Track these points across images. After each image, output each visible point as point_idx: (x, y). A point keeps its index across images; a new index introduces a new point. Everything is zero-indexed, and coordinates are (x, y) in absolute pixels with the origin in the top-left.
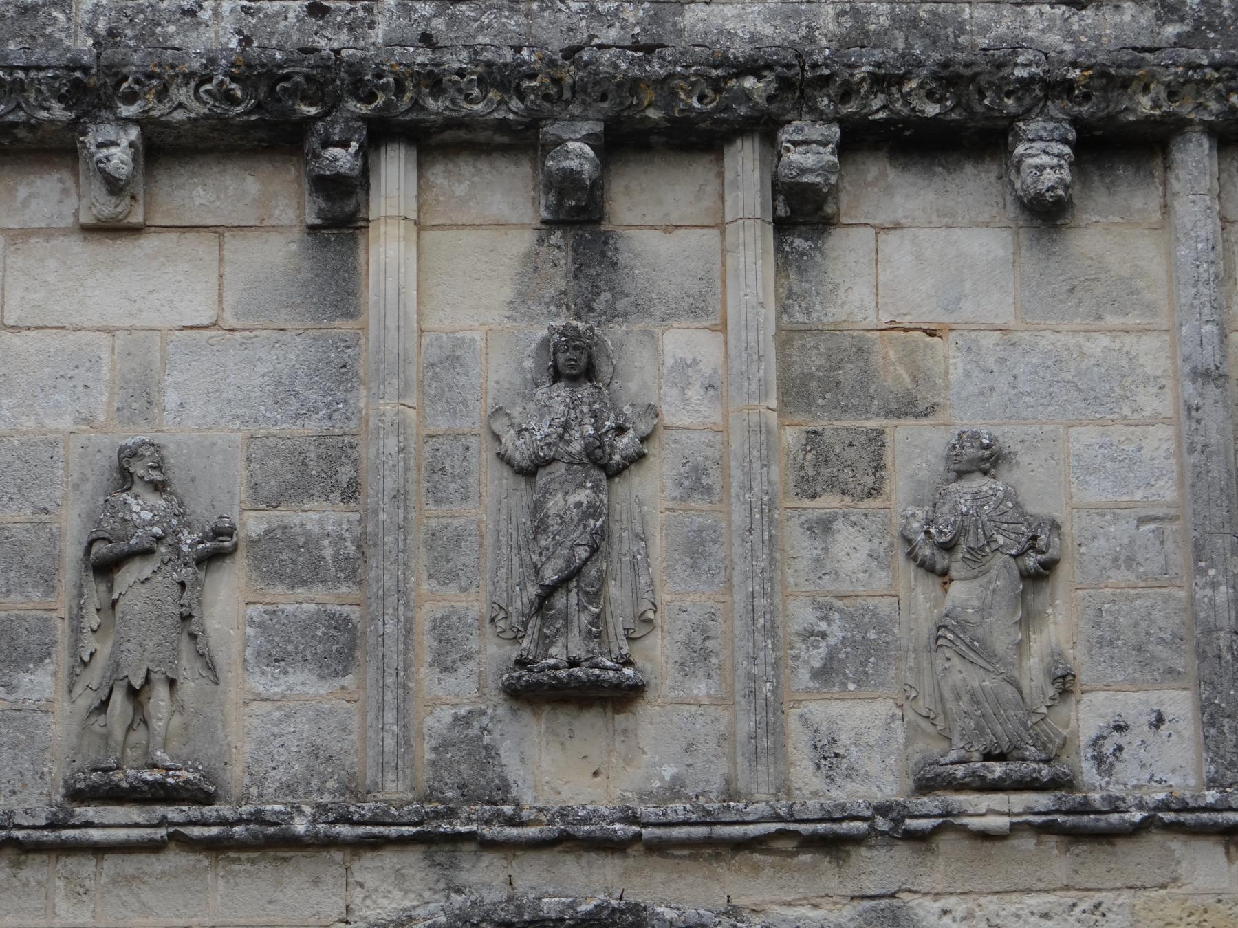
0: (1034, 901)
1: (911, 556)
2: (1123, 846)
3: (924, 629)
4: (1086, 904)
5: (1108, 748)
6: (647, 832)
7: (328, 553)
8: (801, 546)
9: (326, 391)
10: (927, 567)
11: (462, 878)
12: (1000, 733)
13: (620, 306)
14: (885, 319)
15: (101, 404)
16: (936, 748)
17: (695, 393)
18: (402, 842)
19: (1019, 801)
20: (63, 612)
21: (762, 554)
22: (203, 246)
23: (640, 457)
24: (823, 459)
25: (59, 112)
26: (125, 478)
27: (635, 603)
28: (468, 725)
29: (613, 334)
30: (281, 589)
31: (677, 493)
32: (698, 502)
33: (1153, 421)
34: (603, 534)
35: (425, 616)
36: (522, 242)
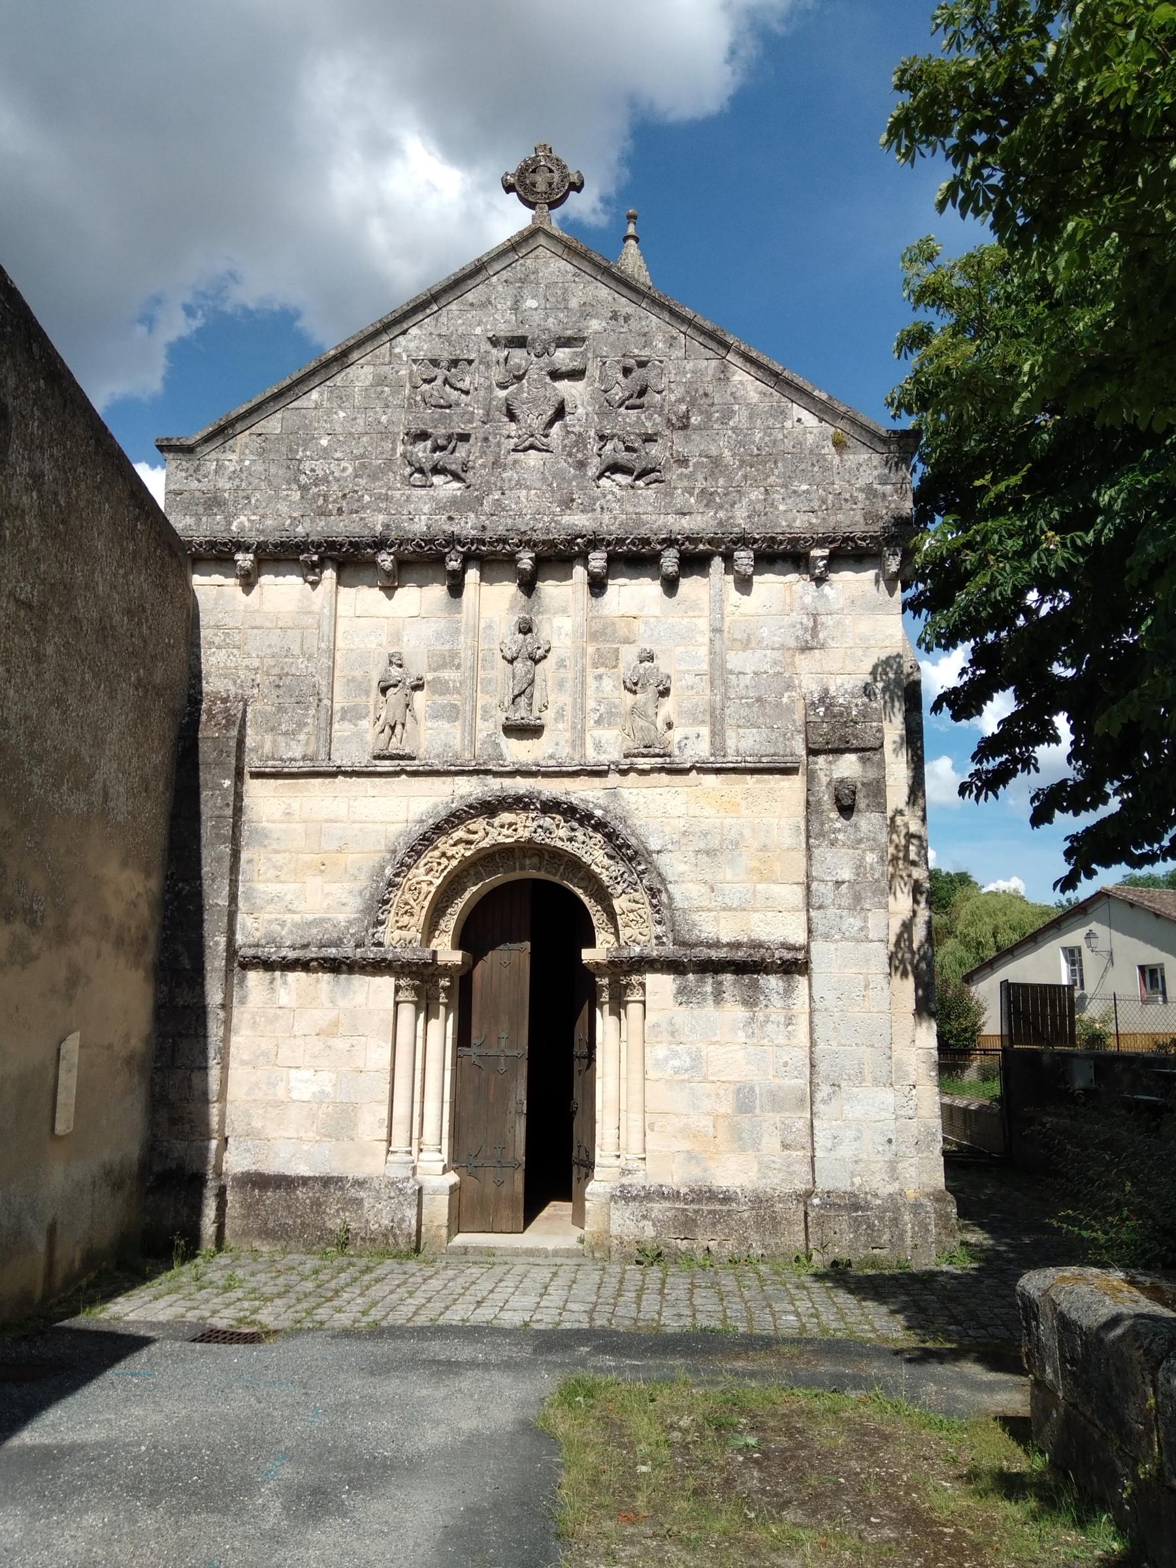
0: (658, 790)
1: (626, 687)
3: (628, 708)
10: (630, 690)
15: (384, 640)
16: (631, 744)
19: (653, 760)
21: (579, 686)
23: (545, 657)
26: (391, 663)
29: (537, 619)
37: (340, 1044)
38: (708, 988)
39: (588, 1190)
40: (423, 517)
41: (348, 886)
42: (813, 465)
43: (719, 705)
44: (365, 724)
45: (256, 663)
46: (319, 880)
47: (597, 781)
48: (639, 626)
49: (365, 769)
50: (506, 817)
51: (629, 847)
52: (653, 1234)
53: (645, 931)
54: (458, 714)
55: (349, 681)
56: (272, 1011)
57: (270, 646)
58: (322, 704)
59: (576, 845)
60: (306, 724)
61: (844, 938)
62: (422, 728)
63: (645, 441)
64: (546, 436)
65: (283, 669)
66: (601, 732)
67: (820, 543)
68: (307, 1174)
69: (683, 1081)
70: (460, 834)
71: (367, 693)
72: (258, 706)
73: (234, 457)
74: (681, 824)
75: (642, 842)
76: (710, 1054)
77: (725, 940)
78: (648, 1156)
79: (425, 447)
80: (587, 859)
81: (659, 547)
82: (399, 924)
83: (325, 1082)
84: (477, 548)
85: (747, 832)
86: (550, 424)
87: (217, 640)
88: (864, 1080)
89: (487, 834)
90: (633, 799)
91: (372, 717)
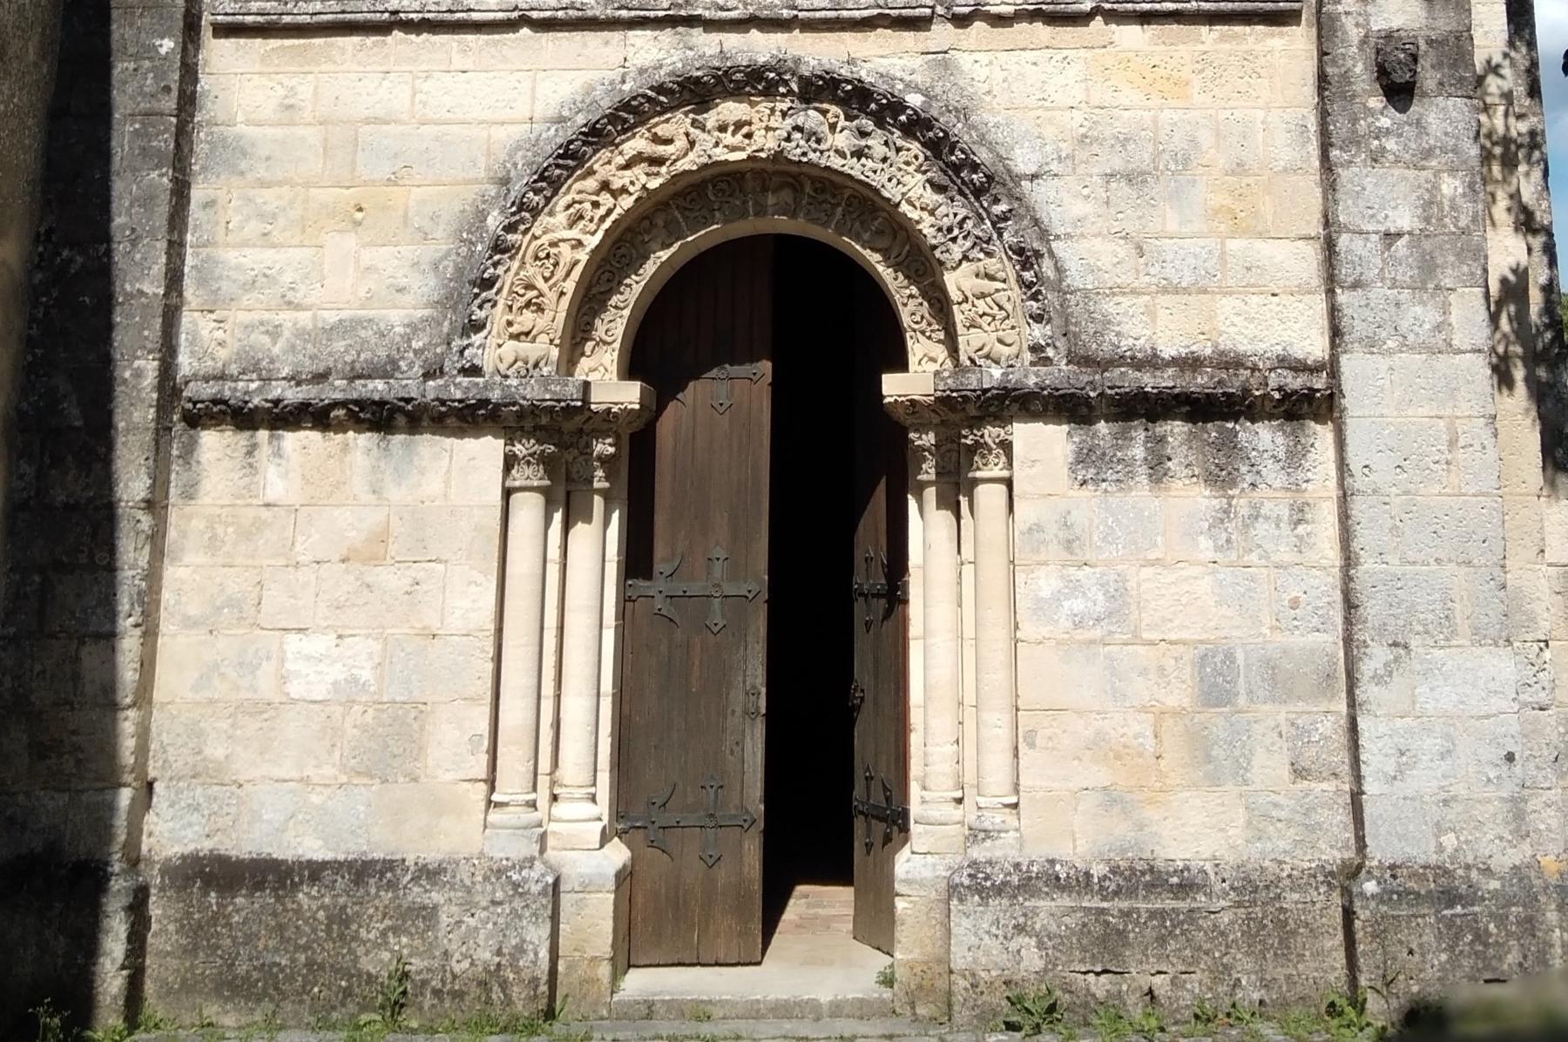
4: (1059, 57)
6: (801, 15)
38: (1138, 451)
46: (350, 241)
47: (908, 38)
49: (448, 16)
50: (730, 110)
51: (975, 167)
53: (1010, 336)
59: (870, 163)
61: (1404, 346)
69: (1092, 642)
75: (1001, 159)
76: (1144, 587)
77: (1167, 352)
80: (891, 192)
82: (514, 329)
85: (1205, 138)
89: (692, 144)
90: (981, 73)
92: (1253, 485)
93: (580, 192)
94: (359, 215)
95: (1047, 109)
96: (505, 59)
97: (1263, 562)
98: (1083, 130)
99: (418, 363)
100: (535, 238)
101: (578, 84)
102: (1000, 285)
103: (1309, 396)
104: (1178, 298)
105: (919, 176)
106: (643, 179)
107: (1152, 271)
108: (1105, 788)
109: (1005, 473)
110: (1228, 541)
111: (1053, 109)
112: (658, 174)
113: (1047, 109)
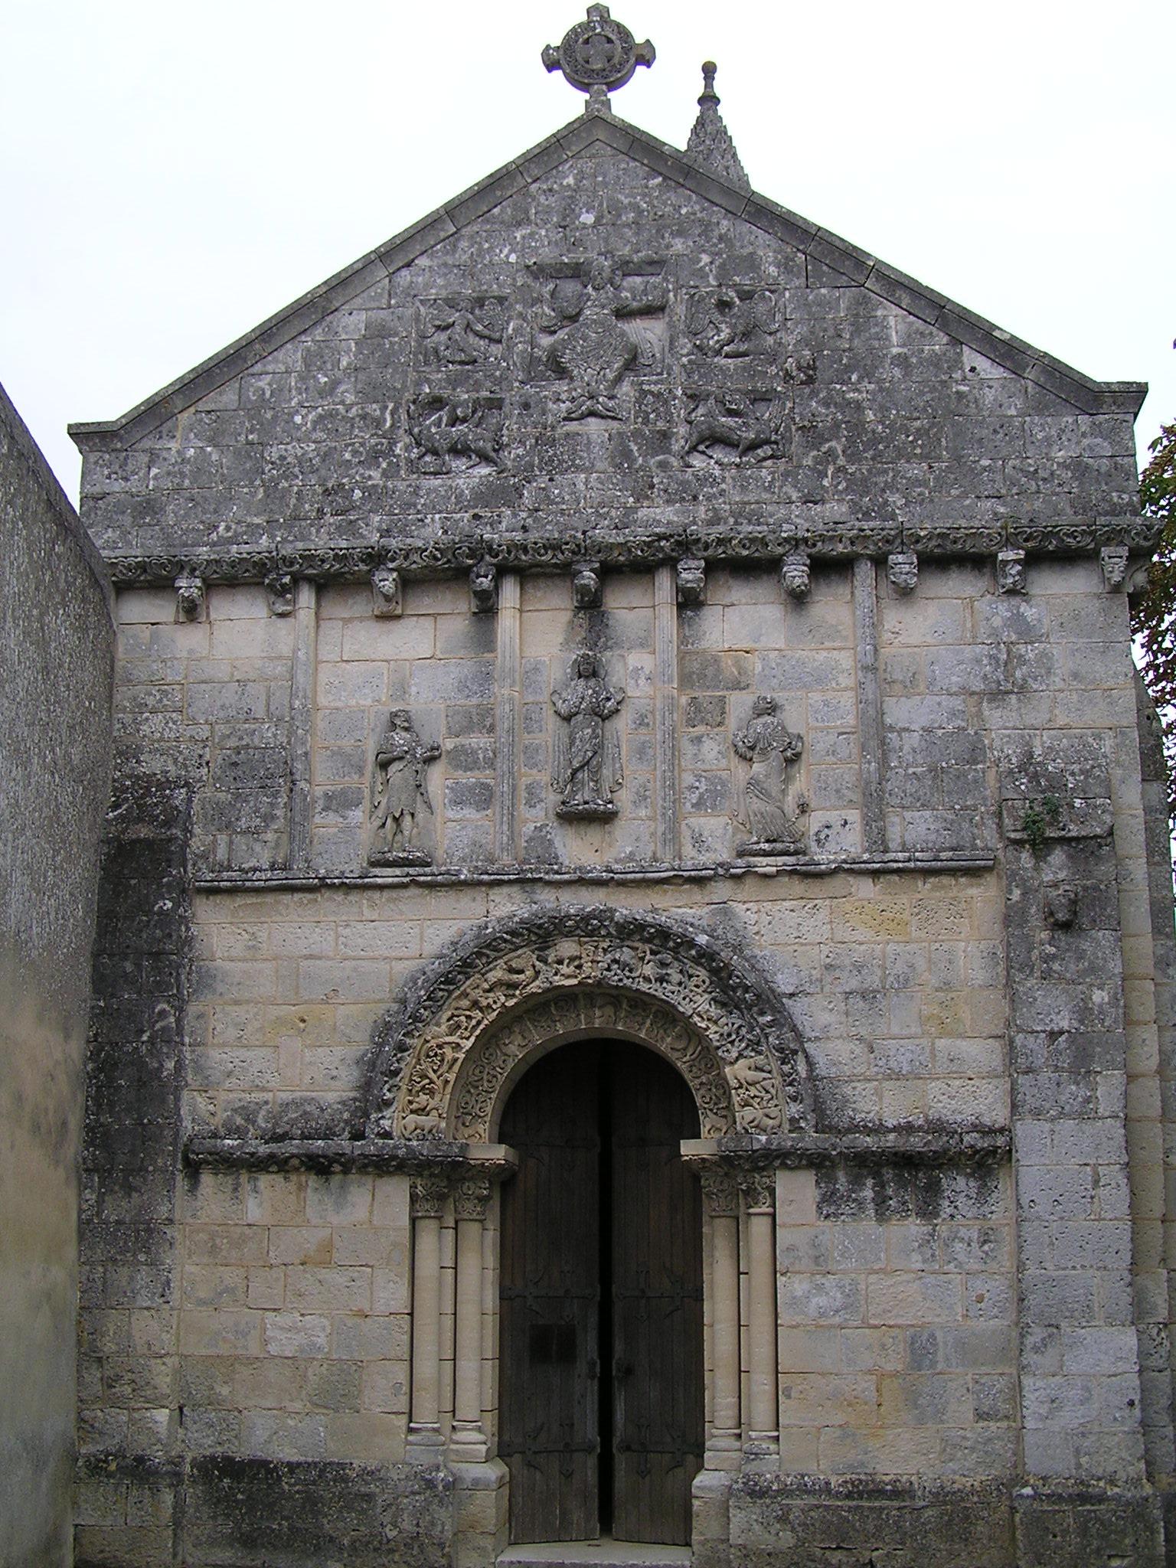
0: (787, 904)
1: (736, 752)
2: (827, 880)
3: (743, 784)
5: (822, 836)
6: (616, 876)
7: (481, 756)
8: (688, 749)
9: (481, 685)
10: (743, 757)
11: (537, 897)
12: (773, 831)
13: (609, 644)
14: (726, 646)
17: (642, 681)
18: (510, 882)
19: (781, 860)
20: (367, 785)
21: (669, 753)
22: (427, 623)
24: (698, 710)
25: (363, 567)
26: (393, 726)
27: (614, 776)
28: (541, 831)
30: (460, 772)
31: (634, 726)
32: (643, 730)
33: (846, 689)
34: (601, 746)
35: (524, 781)
36: (566, 616)
37: (337, 1278)
38: (868, 1193)
39: (696, 1482)
40: (437, 516)
41: (339, 1051)
42: (995, 431)
43: (875, 778)
44: (357, 815)
45: (204, 732)
47: (696, 894)
48: (755, 665)
49: (359, 881)
50: (567, 947)
51: (747, 989)
52: (792, 1542)
53: (774, 1112)
54: (491, 796)
55: (334, 754)
56: (238, 1230)
57: (223, 706)
58: (297, 789)
59: (670, 987)
60: (274, 817)
62: (439, 819)
63: (753, 401)
64: (611, 398)
65: (241, 739)
66: (702, 820)
67: (1009, 542)
68: (295, 1459)
69: (832, 1326)
70: (497, 974)
71: (360, 771)
72: (208, 792)
73: (174, 445)
74: (820, 955)
76: (872, 1288)
77: (890, 1123)
78: (782, 1433)
79: (440, 419)
80: (686, 1008)
81: (780, 550)
82: (414, 1106)
83: (318, 1330)
84: (516, 558)
85: (921, 964)
86: (619, 379)
87: (151, 701)
88: (1093, 1318)
89: (537, 973)
91: (366, 804)
92: (952, 1216)
93: (456, 1009)
94: (302, 1025)
95: (802, 944)
96: (401, 913)
97: (956, 1270)
98: (828, 960)
99: (348, 1129)
100: (428, 1042)
101: (455, 928)
102: (765, 1075)
103: (993, 1152)
104: (898, 1083)
105: (706, 996)
106: (503, 999)
107: (880, 1063)
108: (840, 1426)
109: (770, 1210)
110: (933, 1255)
111: (805, 945)
112: (514, 996)
113: (802, 944)
